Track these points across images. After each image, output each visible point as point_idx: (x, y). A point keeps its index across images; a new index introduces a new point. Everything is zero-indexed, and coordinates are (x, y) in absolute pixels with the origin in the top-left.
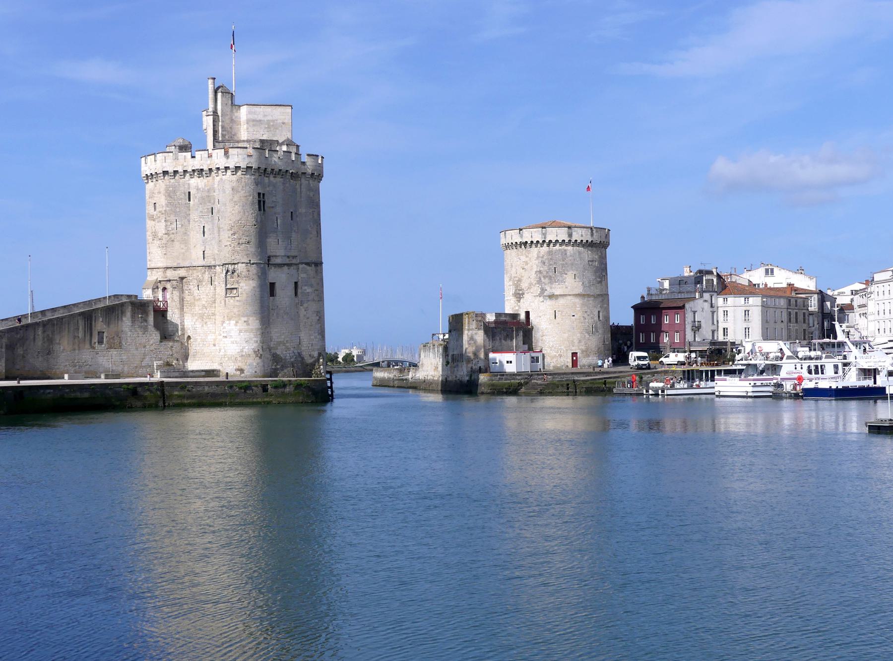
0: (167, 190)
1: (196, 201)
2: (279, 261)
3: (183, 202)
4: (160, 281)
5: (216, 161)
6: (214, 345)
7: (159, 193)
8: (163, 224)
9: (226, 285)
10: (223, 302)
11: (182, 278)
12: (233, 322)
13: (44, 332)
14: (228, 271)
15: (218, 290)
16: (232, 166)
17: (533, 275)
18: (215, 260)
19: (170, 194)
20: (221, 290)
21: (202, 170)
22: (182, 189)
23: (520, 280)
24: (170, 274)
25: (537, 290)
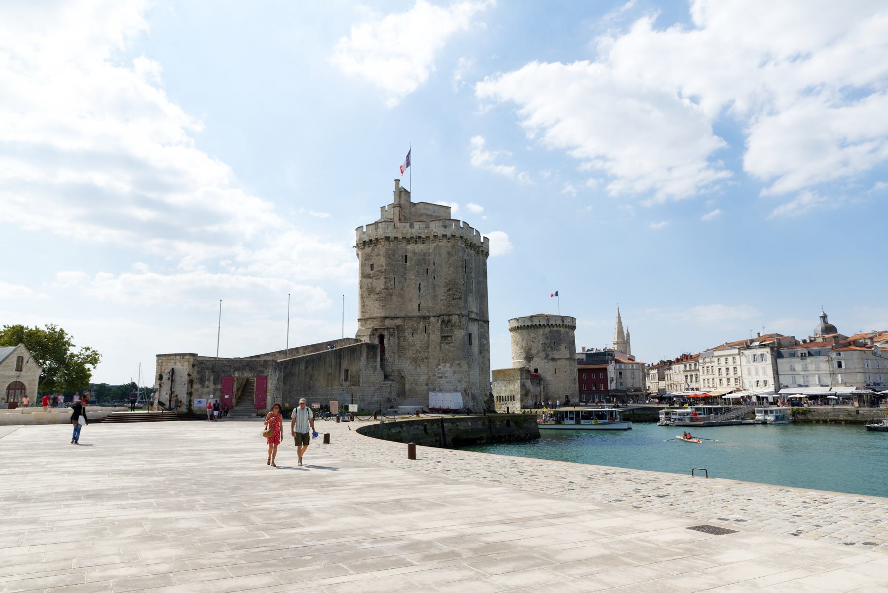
0: (387, 250)
1: (413, 262)
2: (473, 316)
3: (401, 263)
4: (376, 329)
5: (434, 230)
6: (427, 385)
7: (378, 255)
8: (382, 280)
9: (442, 331)
10: (438, 347)
11: (398, 327)
12: (448, 365)
13: (306, 368)
14: (443, 321)
15: (432, 337)
16: (449, 234)
17: (540, 345)
18: (429, 312)
19: (389, 256)
20: (436, 337)
21: (420, 237)
22: (400, 252)
23: (530, 349)
24: (388, 323)
25: (543, 355)
